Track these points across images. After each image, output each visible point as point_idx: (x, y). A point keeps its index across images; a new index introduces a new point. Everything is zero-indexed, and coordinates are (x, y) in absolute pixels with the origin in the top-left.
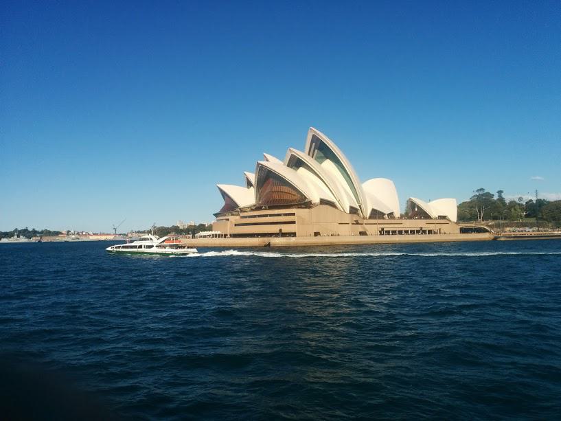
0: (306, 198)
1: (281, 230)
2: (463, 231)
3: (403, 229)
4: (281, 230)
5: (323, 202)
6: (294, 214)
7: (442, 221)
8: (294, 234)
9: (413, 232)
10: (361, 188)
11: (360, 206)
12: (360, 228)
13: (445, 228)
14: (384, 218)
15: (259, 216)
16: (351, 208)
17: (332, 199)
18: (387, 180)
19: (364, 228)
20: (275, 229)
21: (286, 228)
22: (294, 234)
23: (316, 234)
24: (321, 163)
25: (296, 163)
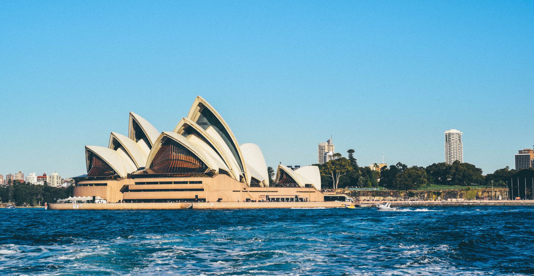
0: (207, 167)
1: (197, 196)
2: (327, 199)
3: (276, 197)
4: (197, 196)
5: (222, 171)
6: (201, 182)
7: (307, 189)
8: (204, 200)
9: (283, 200)
10: (189, 142)
11: (244, 174)
12: (246, 196)
13: (312, 196)
14: (259, 186)
15: (161, 183)
16: (241, 176)
17: (225, 168)
18: (249, 144)
19: (250, 195)
20: (191, 195)
21: (201, 195)
22: (204, 200)
23: (219, 200)
24: (205, 129)
25: (188, 130)
